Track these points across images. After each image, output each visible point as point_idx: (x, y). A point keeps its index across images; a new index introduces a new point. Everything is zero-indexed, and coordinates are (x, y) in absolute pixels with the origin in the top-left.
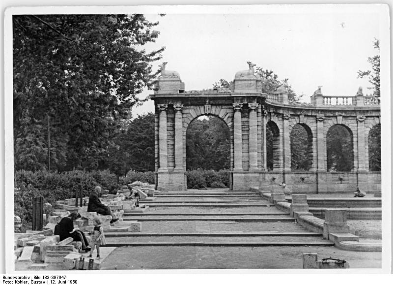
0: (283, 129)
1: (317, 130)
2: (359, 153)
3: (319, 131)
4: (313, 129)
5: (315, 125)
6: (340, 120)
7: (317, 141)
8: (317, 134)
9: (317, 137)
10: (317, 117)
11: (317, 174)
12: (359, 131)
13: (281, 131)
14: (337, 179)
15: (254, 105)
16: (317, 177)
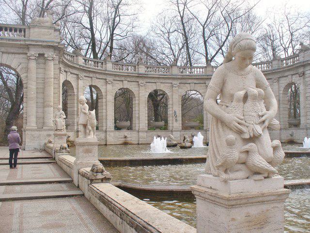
0: (78, 89)
1: (106, 92)
2: (140, 114)
3: (108, 93)
4: (103, 90)
5: (104, 87)
6: (126, 85)
7: (106, 102)
8: (106, 95)
9: (106, 99)
10: (107, 80)
11: (106, 132)
12: (141, 94)
13: (75, 90)
14: (123, 136)
15: (50, 53)
16: (106, 135)
